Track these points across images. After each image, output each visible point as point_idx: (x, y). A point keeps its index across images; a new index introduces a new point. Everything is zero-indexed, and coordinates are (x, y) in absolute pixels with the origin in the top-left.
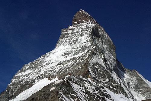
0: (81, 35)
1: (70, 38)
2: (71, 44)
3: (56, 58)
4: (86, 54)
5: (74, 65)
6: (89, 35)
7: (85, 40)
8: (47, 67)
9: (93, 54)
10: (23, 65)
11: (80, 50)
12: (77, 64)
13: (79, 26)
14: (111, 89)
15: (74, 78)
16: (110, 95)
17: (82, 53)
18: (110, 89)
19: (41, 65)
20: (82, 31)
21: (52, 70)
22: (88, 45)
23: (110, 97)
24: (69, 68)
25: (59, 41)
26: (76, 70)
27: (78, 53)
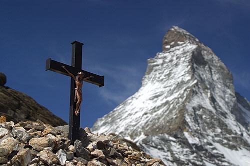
0: (177, 65)
1: (160, 71)
2: (162, 80)
3: (142, 105)
4: (184, 93)
5: (166, 113)
6: (187, 64)
7: (182, 72)
8: (128, 121)
9: (193, 93)
10: (95, 121)
11: (175, 89)
12: (171, 112)
13: (173, 51)
14: (225, 144)
15: (154, 138)
16: (223, 155)
17: (178, 93)
18: (223, 145)
19: (119, 117)
20: (177, 59)
21: (134, 123)
22: (186, 80)
23: (224, 158)
24: (159, 118)
25: (145, 78)
26: (168, 122)
27: (172, 93)
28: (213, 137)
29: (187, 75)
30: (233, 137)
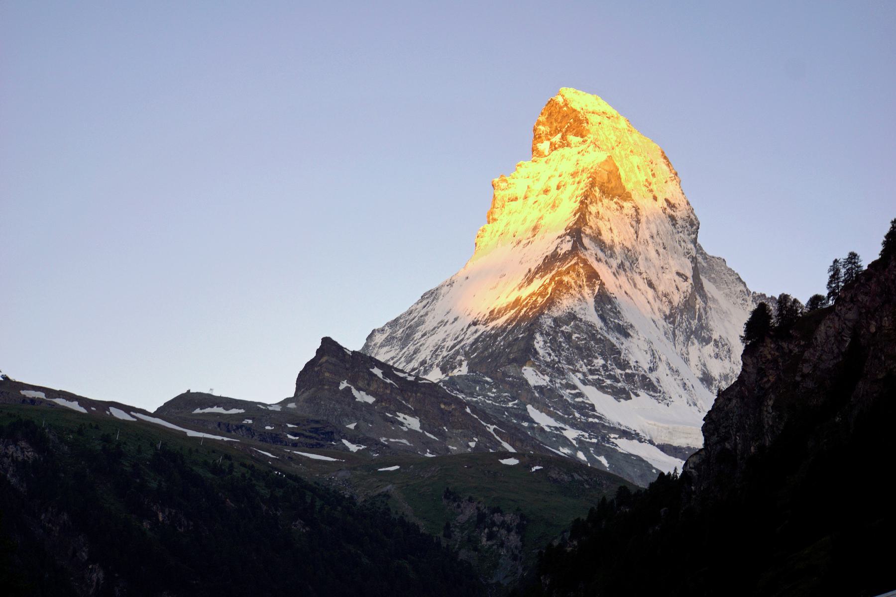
11: (539, 269)
20: (558, 188)
28: (584, 374)
29: (568, 238)
30: (627, 375)
